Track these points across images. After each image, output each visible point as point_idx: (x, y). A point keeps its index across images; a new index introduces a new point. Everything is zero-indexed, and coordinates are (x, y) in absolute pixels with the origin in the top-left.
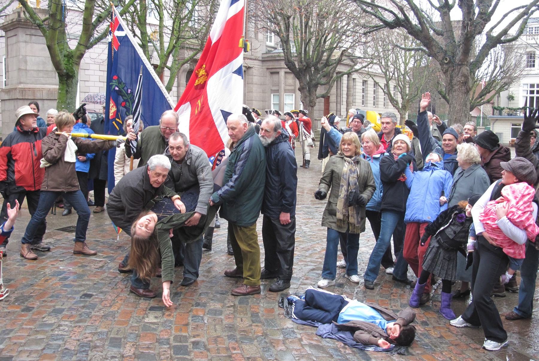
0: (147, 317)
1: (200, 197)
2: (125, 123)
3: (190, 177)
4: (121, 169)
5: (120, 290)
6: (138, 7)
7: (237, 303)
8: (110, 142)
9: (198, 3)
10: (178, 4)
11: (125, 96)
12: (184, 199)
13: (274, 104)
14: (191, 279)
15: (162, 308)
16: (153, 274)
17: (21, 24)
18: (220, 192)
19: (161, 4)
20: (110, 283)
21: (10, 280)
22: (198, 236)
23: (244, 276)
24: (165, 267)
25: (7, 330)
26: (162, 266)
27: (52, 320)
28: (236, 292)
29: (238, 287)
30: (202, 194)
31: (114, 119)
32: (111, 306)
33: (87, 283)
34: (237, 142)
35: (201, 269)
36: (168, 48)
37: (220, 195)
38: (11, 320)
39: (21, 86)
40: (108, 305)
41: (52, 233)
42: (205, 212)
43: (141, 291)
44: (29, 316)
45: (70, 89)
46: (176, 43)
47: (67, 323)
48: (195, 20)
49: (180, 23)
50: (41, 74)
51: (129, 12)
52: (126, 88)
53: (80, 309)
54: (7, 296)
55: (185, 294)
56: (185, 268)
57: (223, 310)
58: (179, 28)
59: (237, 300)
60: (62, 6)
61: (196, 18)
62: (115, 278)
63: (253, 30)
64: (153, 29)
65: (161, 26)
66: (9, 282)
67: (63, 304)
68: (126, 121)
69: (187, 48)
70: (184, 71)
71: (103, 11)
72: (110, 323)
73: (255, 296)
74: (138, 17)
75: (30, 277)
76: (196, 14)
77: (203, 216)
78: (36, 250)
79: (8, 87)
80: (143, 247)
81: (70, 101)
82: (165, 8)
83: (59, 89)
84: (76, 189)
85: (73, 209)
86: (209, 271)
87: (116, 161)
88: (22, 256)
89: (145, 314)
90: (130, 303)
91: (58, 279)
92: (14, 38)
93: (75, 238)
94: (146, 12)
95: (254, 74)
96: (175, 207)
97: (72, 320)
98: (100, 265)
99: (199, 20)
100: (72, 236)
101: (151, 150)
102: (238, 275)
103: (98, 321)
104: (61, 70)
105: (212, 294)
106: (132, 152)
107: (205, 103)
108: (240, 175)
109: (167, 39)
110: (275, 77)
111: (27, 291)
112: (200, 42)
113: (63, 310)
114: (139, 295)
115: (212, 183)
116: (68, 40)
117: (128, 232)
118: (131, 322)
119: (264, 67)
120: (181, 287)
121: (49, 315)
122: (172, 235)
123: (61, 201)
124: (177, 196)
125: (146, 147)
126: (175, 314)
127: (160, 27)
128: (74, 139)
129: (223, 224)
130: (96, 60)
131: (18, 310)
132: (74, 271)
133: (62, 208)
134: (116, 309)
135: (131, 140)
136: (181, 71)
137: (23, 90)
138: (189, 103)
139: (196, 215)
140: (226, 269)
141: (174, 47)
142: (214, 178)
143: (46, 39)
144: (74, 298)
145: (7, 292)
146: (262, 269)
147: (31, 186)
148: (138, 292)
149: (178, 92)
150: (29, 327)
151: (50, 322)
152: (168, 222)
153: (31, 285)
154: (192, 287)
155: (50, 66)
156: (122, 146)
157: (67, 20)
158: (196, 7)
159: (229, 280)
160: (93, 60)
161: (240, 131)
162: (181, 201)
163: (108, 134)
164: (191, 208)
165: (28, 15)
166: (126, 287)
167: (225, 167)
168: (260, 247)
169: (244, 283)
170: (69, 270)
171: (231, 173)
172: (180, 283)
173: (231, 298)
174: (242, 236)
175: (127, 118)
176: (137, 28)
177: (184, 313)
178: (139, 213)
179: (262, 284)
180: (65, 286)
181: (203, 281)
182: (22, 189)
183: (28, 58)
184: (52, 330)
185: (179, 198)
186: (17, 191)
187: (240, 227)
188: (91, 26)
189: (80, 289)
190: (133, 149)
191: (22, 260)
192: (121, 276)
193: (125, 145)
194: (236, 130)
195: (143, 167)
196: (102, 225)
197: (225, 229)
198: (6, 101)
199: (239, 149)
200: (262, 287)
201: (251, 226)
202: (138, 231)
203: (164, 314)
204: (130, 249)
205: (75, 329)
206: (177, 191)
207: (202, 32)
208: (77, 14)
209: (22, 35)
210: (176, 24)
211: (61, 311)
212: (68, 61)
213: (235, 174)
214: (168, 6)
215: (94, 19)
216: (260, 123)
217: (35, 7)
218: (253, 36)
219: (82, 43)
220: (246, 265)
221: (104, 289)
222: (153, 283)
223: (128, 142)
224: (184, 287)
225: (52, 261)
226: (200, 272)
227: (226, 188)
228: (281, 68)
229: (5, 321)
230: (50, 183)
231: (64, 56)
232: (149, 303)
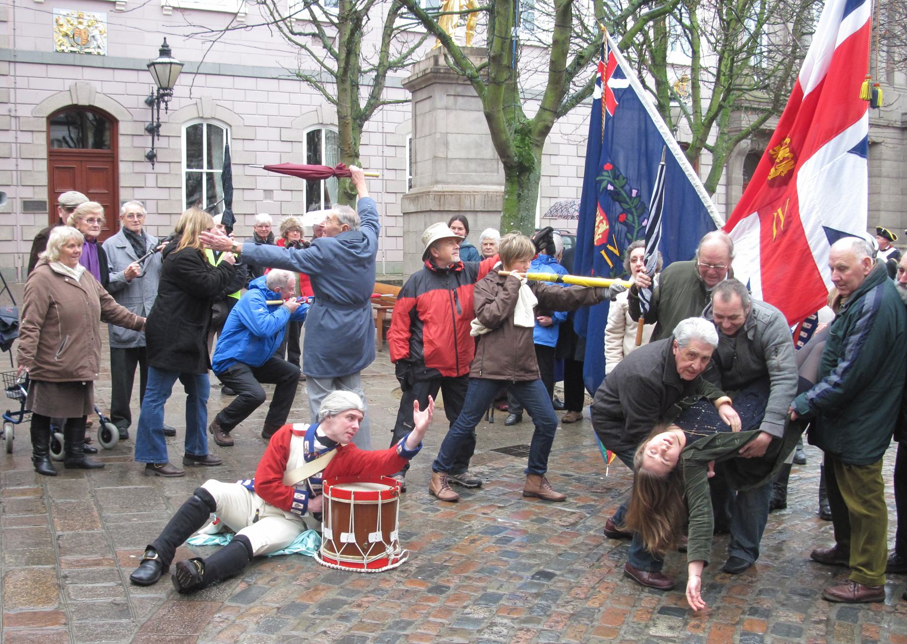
0: (655, 625)
1: (770, 401)
2: (626, 254)
3: (752, 363)
4: (618, 342)
5: (606, 570)
6: (651, 34)
7: (833, 615)
8: (598, 290)
9: (768, 18)
10: (728, 23)
11: (627, 203)
12: (739, 404)
14: (742, 561)
15: (684, 611)
16: (672, 546)
17: (439, 78)
18: (811, 394)
19: (695, 24)
20: (587, 556)
21: (411, 535)
22: (764, 477)
23: (851, 563)
24: (694, 533)
25: (402, 621)
26: (690, 531)
27: (480, 613)
28: (833, 595)
29: (836, 585)
30: (775, 398)
31: (603, 246)
32: (587, 598)
33: (547, 551)
34: (849, 295)
35: (765, 544)
36: (709, 110)
37: (812, 399)
38: (410, 604)
39: (438, 188)
40: (582, 596)
41: (485, 457)
42: (779, 432)
43: (645, 575)
44: (440, 601)
45: (526, 191)
46: (724, 100)
47: (505, 621)
48: (761, 53)
49: (733, 59)
50: (473, 166)
51: (633, 44)
52: (627, 187)
53: (530, 598)
54: (404, 563)
55: (729, 590)
56: (732, 537)
57: (803, 626)
58: (731, 70)
59: (834, 611)
60: (512, 41)
61: (764, 49)
62: (597, 546)
63: (884, 65)
64: (680, 74)
65: (695, 68)
66: (409, 538)
67: (501, 586)
68: (630, 252)
69: (746, 108)
70: (739, 153)
71: (585, 45)
72: (584, 628)
73: (873, 606)
74: (651, 52)
75: (444, 532)
76: (764, 42)
77: (775, 439)
78: (456, 485)
79: (413, 190)
80: (656, 493)
81: (524, 214)
82: (703, 33)
83: (506, 192)
84: (532, 377)
85: (525, 414)
86: (778, 548)
87: (608, 327)
88: (432, 493)
89: (651, 619)
90: (624, 596)
91: (493, 540)
92: (428, 101)
93: (526, 467)
94: (666, 43)
95: (884, 157)
96: (721, 420)
97: (515, 616)
98: (572, 520)
99: (770, 51)
100: (523, 463)
101: (678, 307)
102: (837, 562)
103: (562, 624)
104: (508, 157)
105: (784, 593)
106: (642, 310)
107: (793, 215)
108: (853, 362)
109: (706, 92)
111: (438, 557)
112: (772, 96)
113: (500, 597)
114: (642, 583)
115: (795, 375)
116: (522, 101)
117: (628, 462)
118: (622, 632)
120: (723, 574)
121: (476, 602)
122: (712, 473)
123: (504, 399)
124: (725, 398)
125: (669, 302)
126: (708, 625)
127: (693, 70)
128: (532, 284)
129: (811, 457)
130: (570, 137)
131: (423, 588)
132: (523, 527)
133: (505, 410)
134: (596, 605)
135: (640, 288)
136: (734, 154)
137: (440, 196)
138: (755, 214)
139: (762, 437)
140: (814, 547)
141: (721, 107)
142: (800, 364)
143: (484, 102)
144: (521, 578)
145: (405, 555)
146: (889, 554)
147: (451, 369)
148: (640, 577)
149: (728, 194)
150: (439, 620)
151: (476, 616)
152: (705, 448)
153: (447, 546)
154: (745, 577)
155: (489, 151)
156: (623, 299)
157: (520, 65)
158: (765, 27)
159: (820, 569)
160: (566, 137)
161: (856, 273)
162: (733, 407)
163: (590, 276)
164: (752, 422)
165: (451, 60)
166: (616, 566)
167: (822, 344)
168: (889, 509)
169: (851, 577)
170: (514, 525)
171: (834, 357)
172: (721, 567)
173: (821, 606)
174: (851, 483)
175: (631, 246)
176: (649, 75)
177: (727, 625)
178: (652, 427)
179: (888, 585)
180: (506, 553)
181: (767, 567)
182: (434, 374)
183: (451, 138)
184: (479, 631)
185: (728, 403)
186: (426, 377)
187: (849, 465)
188: (564, 74)
189: (532, 562)
190: (643, 305)
191: (432, 501)
192: (609, 544)
193: (630, 297)
194: (848, 272)
195: (662, 342)
196: (577, 447)
197: (814, 468)
198: (411, 216)
199: (854, 310)
200: (887, 590)
201: (872, 464)
202: (648, 462)
203: (686, 624)
204: (629, 494)
205: (520, 634)
206: (726, 390)
207: (775, 77)
208: (536, 52)
209: (441, 97)
210: (724, 63)
211: (495, 598)
212: (523, 140)
213: (844, 360)
214: (709, 29)
215: (570, 60)
216: (896, 255)
217: (464, 45)
218: (883, 79)
219: (547, 106)
220: (857, 543)
221: (577, 566)
222: (669, 561)
223: (635, 290)
224: (728, 575)
225: (483, 507)
226: (762, 549)
227: (824, 386)
229: (400, 606)
230: (487, 364)
231: (516, 132)
232: (659, 600)
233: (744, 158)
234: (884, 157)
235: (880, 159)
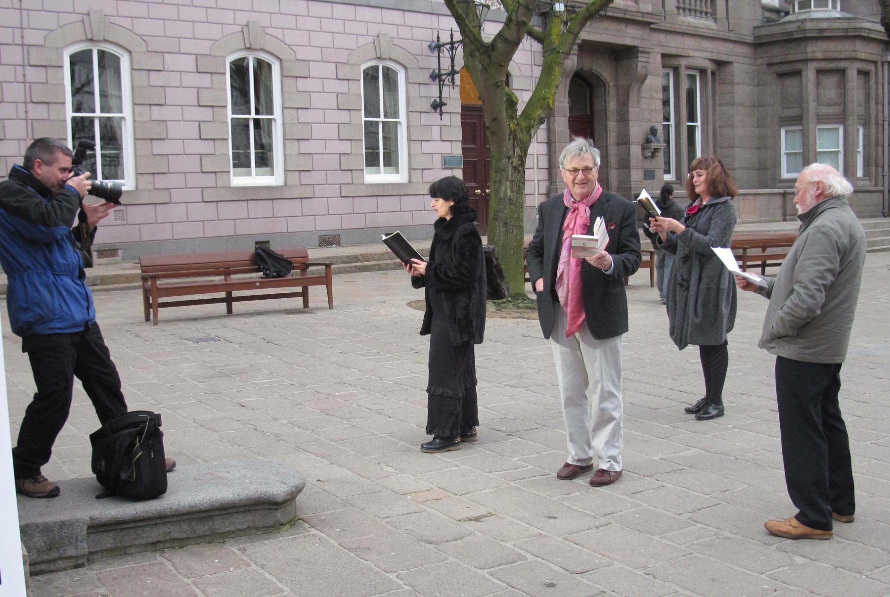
13: (788, 154)
110: (791, 84)
119: (759, 61)
228: (806, 61)
233: (569, 80)
234: (737, 80)
235: (732, 83)
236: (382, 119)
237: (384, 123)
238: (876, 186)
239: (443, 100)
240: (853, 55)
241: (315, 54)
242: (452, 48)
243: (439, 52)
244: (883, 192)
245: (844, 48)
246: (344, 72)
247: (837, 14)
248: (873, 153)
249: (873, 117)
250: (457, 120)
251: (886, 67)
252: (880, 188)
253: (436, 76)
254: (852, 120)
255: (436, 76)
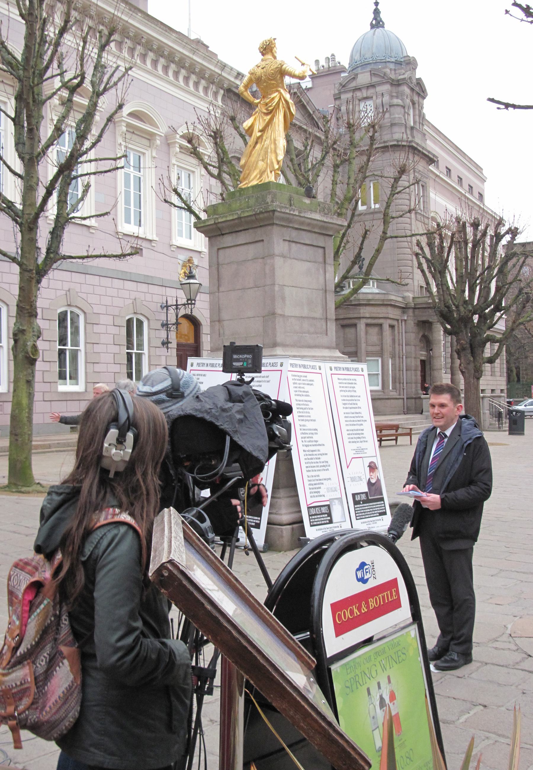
110: (350, 331)
228: (360, 318)
236: (135, 351)
237: (135, 353)
238: (400, 395)
239: (169, 340)
240: (386, 316)
241: (102, 310)
242: (177, 308)
243: (167, 310)
244: (403, 399)
245: (381, 311)
246: (118, 322)
247: (377, 291)
248: (398, 375)
249: (397, 353)
250: (174, 352)
251: (403, 323)
252: (402, 397)
253: (165, 325)
254: (386, 355)
255: (165, 325)
